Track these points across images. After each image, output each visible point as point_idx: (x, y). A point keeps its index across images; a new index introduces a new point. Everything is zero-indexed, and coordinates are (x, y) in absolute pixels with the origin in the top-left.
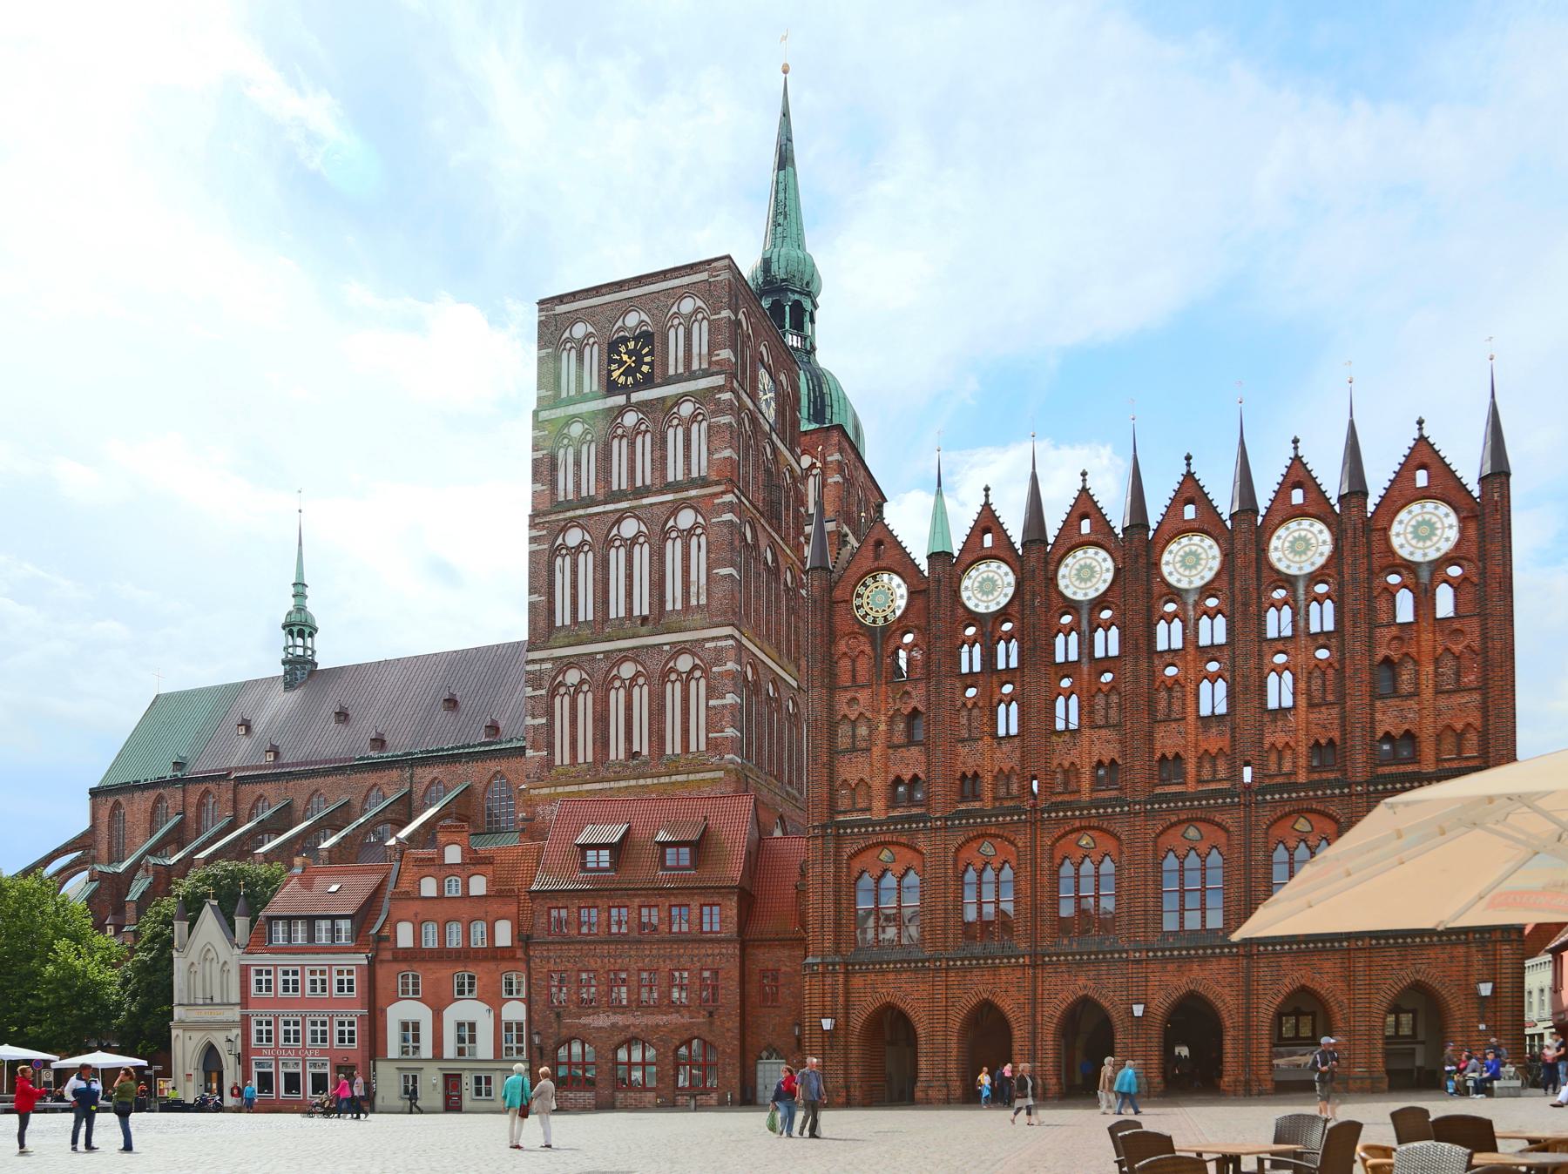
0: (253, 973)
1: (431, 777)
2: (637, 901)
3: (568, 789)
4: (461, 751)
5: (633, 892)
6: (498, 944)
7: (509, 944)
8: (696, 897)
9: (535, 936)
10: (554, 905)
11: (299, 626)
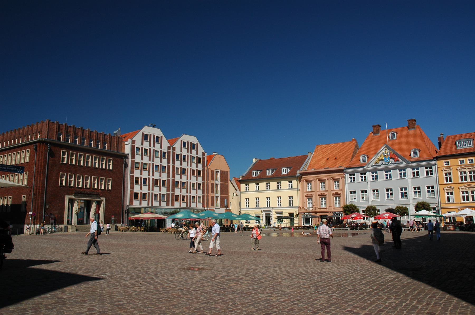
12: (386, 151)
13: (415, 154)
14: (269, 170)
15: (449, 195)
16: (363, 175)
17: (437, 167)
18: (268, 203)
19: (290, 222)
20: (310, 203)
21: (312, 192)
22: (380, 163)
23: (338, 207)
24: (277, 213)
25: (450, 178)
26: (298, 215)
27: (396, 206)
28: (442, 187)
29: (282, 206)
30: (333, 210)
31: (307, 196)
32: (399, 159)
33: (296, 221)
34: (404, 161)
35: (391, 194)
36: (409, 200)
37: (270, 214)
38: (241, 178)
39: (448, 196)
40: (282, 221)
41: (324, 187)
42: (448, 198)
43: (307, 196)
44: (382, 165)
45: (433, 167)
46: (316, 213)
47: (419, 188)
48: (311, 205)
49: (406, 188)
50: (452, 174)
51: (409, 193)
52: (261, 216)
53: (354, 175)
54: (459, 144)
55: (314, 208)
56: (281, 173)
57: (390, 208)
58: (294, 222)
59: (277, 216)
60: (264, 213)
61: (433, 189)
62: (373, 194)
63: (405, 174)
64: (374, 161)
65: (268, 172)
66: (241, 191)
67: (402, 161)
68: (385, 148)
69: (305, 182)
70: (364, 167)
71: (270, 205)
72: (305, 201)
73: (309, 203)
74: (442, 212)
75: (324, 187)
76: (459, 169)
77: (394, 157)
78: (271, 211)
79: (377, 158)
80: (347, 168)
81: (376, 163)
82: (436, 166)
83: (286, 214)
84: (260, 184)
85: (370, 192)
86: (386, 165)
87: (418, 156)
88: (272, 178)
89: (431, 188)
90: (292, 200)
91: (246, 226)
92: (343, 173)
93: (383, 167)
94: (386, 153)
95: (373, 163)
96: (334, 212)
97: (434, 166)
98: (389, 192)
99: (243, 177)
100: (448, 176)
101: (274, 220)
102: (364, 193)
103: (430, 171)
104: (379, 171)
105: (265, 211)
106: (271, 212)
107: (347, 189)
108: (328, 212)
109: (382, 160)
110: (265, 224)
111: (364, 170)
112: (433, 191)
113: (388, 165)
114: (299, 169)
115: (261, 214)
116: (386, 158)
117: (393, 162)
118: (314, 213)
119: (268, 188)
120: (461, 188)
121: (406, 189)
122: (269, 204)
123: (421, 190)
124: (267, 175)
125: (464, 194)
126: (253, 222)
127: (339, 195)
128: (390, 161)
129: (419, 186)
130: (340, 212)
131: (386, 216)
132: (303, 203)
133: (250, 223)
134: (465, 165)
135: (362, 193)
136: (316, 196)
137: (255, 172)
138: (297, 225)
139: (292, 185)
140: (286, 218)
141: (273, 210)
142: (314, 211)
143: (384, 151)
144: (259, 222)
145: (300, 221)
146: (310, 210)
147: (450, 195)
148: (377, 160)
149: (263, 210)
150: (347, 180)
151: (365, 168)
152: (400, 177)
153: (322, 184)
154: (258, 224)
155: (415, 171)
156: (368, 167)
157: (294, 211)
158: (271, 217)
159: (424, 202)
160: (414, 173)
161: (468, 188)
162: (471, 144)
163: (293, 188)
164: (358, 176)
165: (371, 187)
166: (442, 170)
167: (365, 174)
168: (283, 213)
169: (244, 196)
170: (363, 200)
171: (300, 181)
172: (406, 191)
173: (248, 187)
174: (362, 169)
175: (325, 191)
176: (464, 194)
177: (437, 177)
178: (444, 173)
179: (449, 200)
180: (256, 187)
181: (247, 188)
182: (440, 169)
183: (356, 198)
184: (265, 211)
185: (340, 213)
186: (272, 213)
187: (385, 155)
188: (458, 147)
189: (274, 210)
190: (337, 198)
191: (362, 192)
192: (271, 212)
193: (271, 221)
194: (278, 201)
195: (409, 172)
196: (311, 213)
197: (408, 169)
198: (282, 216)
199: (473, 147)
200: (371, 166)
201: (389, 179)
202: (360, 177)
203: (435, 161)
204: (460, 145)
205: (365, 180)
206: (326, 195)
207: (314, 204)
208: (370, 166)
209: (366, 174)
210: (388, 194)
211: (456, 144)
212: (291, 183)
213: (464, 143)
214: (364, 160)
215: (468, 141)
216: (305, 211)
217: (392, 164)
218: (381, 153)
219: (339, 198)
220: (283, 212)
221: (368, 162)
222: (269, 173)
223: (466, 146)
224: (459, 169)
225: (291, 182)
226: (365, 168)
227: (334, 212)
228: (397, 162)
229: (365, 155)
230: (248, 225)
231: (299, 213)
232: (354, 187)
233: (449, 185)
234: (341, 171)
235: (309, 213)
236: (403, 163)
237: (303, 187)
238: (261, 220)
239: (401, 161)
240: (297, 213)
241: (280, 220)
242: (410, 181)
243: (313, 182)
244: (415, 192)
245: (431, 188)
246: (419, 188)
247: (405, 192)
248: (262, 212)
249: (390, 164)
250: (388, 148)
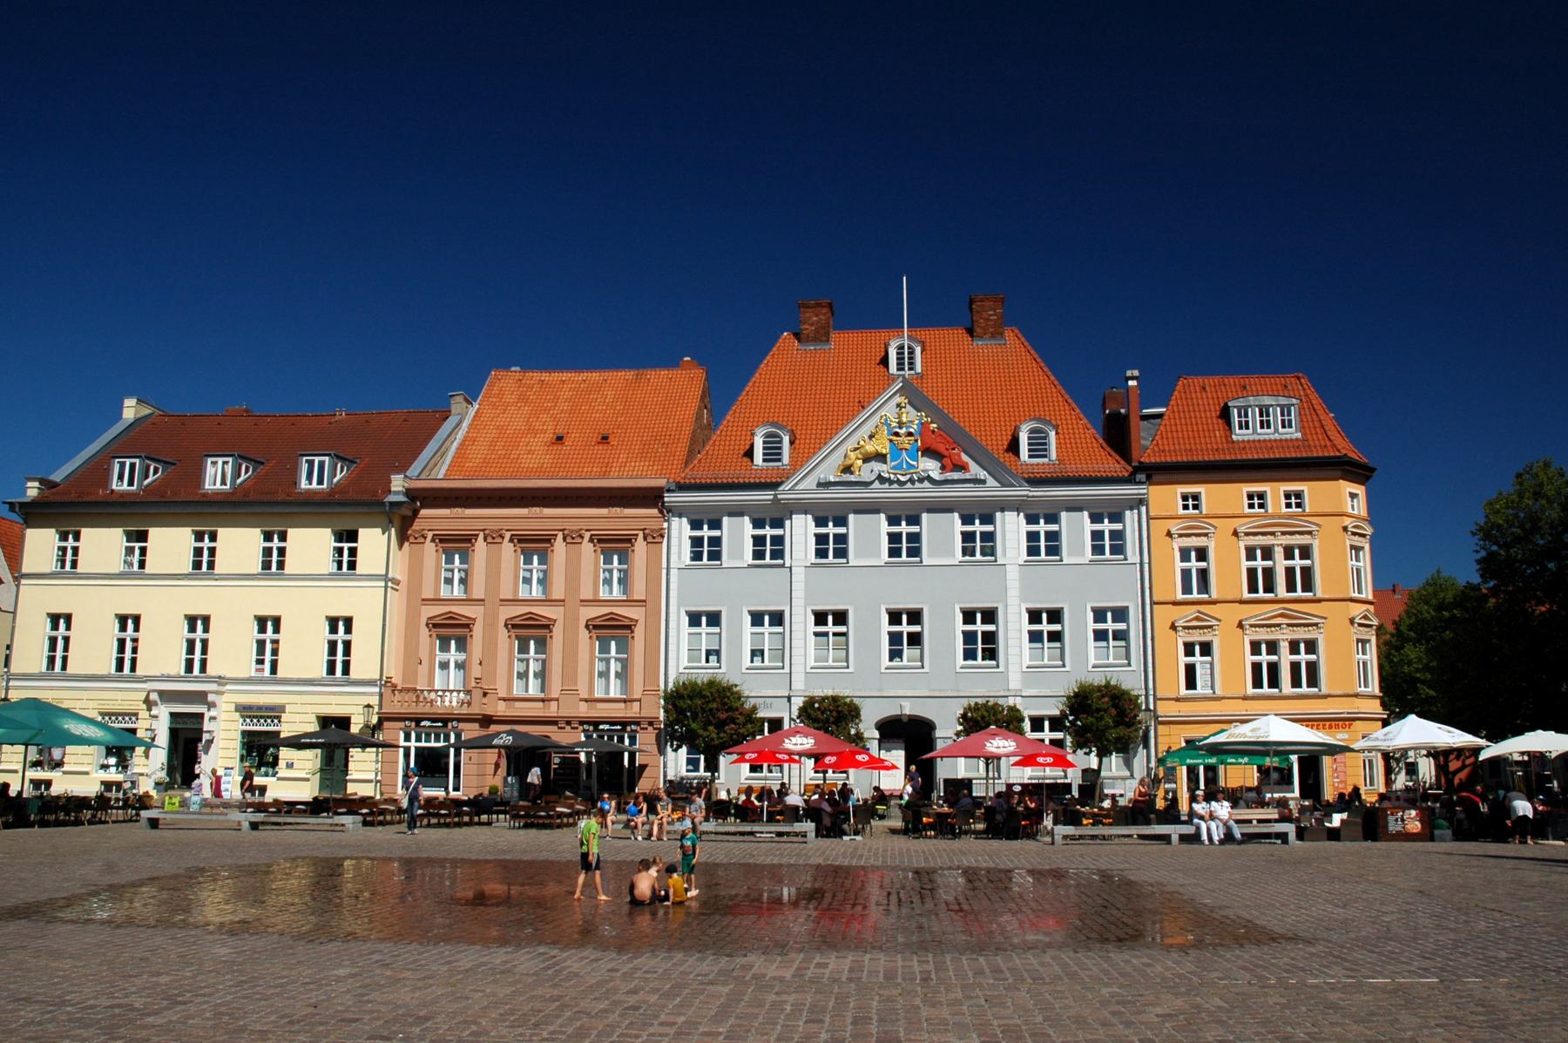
12: (900, 416)
13: (1038, 448)
14: (220, 461)
15: (1193, 655)
16: (768, 532)
17: (1149, 518)
18: (196, 653)
19: (321, 770)
20: (452, 665)
22: (867, 472)
23: (612, 695)
24: (245, 711)
25: (1307, 573)
26: (378, 727)
27: (965, 702)
28: (1165, 615)
29: (281, 674)
30: (584, 710)
31: (435, 626)
32: (965, 458)
33: (360, 766)
34: (989, 473)
35: (915, 639)
36: (1005, 674)
37: (201, 716)
38: (33, 490)
39: (1190, 659)
40: (275, 763)
41: (463, 581)
42: (1190, 670)
43: (435, 626)
44: (877, 484)
45: (1128, 513)
46: (486, 721)
47: (1055, 616)
48: (454, 678)
49: (1127, 607)
50: (1211, 554)
51: (1006, 639)
52: (142, 726)
53: (715, 524)
54: (1240, 416)
55: (477, 694)
56: (295, 483)
57: (907, 711)
58: (346, 771)
59: (245, 734)
60: (163, 712)
61: (1121, 626)
62: (816, 634)
63: (988, 537)
64: (836, 460)
65: (210, 470)
66: (25, 570)
67: (983, 474)
68: (898, 399)
69: (430, 547)
70: (779, 484)
71: (65, 659)
72: (424, 653)
73: (444, 666)
74: (1160, 739)
75: (463, 581)
76: (1247, 534)
77: (941, 448)
78: (211, 698)
79: (851, 444)
80: (682, 488)
81: (847, 469)
82: (1143, 509)
83: (299, 719)
84: (156, 534)
85: (802, 624)
86: (895, 486)
87: (1054, 455)
88: (233, 508)
89: (1050, 622)
90: (347, 645)
91: (36, 784)
92: (655, 511)
93: (879, 492)
94: (901, 425)
95: (828, 469)
96: (589, 723)
97: (1131, 509)
98: (905, 628)
99: (46, 484)
100: (1194, 564)
101: (222, 753)
102: (767, 629)
103: (1047, 533)
104: (857, 512)
105: (167, 696)
106: (211, 705)
107: (673, 601)
108: (554, 723)
109: (881, 458)
110: (162, 775)
111: (776, 500)
112: (1120, 636)
113: (909, 485)
114: (402, 469)
115: (144, 714)
116: (898, 450)
117: (936, 475)
118: (476, 725)
119: (203, 563)
120: (1251, 626)
121: (990, 616)
122: (197, 656)
123: (1068, 627)
124: (207, 487)
125: (1299, 653)
126: (87, 759)
127: (547, 627)
128: (922, 466)
129: (994, 605)
130: (624, 724)
131: (799, 748)
132: (411, 660)
133: (66, 768)
134: (1273, 517)
135: (753, 624)
136: (490, 626)
137: (133, 466)
138: (366, 791)
139: (353, 552)
140: (297, 743)
141: (221, 693)
142: (476, 710)
143: (889, 411)
144: (123, 764)
145: (387, 768)
146: (452, 702)
147: (1197, 659)
148: (852, 455)
149: (161, 693)
150: (674, 550)
151: (786, 492)
152: (965, 552)
153: (528, 561)
154: (113, 775)
155: (1042, 527)
156: (803, 486)
157: (356, 707)
158: (206, 737)
159: (1113, 683)
160: (1032, 537)
161: (1279, 625)
162: (1290, 421)
163: (360, 569)
164: (738, 534)
165: (806, 598)
166: (1169, 534)
167: (778, 523)
168: (284, 717)
169: (37, 602)
170: (755, 664)
171: (403, 538)
172: (916, 628)
173: (76, 550)
174: (766, 496)
175: (630, 602)
176: (1299, 653)
177: (1146, 567)
178: (1242, 545)
179: (1191, 683)
180: (130, 551)
181: (69, 552)
182: (1159, 528)
183: (718, 653)
184: (167, 696)
185: (624, 730)
186: (213, 713)
187: (897, 434)
188: (1238, 431)
189: (226, 697)
190: (453, 642)
191: (757, 619)
192: (211, 705)
193: (204, 758)
194: (261, 645)
195: (1012, 529)
196: (459, 720)
197: (1010, 516)
198: (277, 733)
199: (1299, 435)
200: (820, 485)
201: (978, 556)
202: (689, 542)
203: (1142, 483)
204: (1247, 422)
205: (778, 554)
206: (548, 626)
207: (476, 671)
208: (810, 483)
209: (788, 523)
210: (895, 639)
211: (1225, 414)
212: (346, 546)
213: (1282, 415)
214: (772, 453)
215: (1278, 409)
216: (427, 709)
217: (926, 484)
218: (875, 420)
219: (542, 645)
220: (282, 708)
221: (797, 464)
222: (217, 475)
223: (1250, 431)
224: (1247, 534)
225: (352, 536)
226: (786, 492)
227: (589, 723)
228: (956, 476)
229: (781, 427)
230: (48, 783)
231: (381, 721)
232: (708, 587)
233: (1201, 608)
234: (650, 497)
235: (445, 721)
236: (984, 482)
237: (415, 569)
238: (139, 750)
239: (975, 470)
240: (375, 720)
241: (261, 755)
242: (1013, 574)
243: (480, 544)
244: (1035, 637)
245: (1050, 622)
246: (1055, 616)
247: (909, 634)
248: (149, 704)
249: (921, 480)
250: (914, 395)
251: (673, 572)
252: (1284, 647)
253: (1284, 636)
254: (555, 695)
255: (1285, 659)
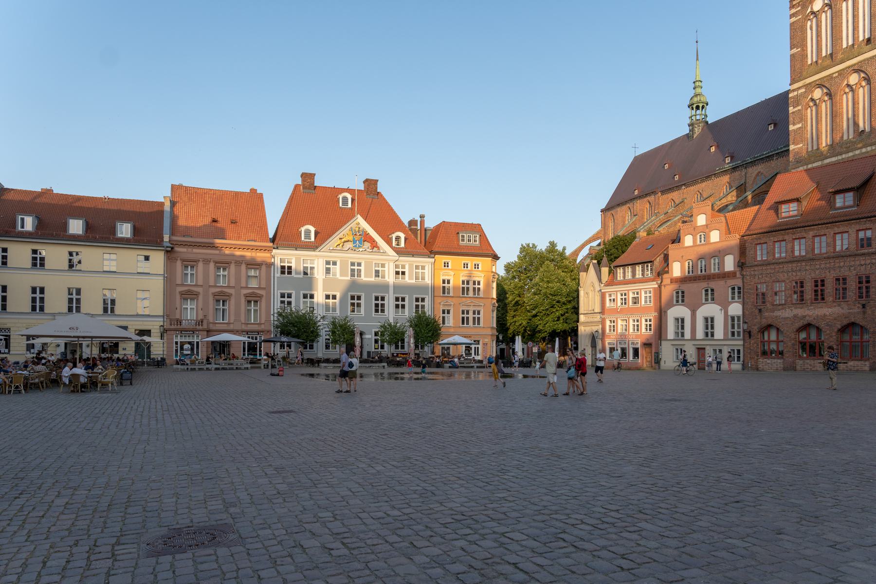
0: (607, 295)
1: (757, 172)
2: (811, 233)
3: (815, 165)
4: (774, 153)
5: (808, 228)
6: (726, 270)
7: (733, 269)
8: (853, 226)
9: (747, 262)
10: (758, 242)
11: (696, 106)
21: (196, 285)
42: (444, 318)
72: (178, 305)
121: (383, 299)
251: (276, 278)
252: (471, 313)
253: (471, 309)
254: (232, 322)
255: (471, 316)
